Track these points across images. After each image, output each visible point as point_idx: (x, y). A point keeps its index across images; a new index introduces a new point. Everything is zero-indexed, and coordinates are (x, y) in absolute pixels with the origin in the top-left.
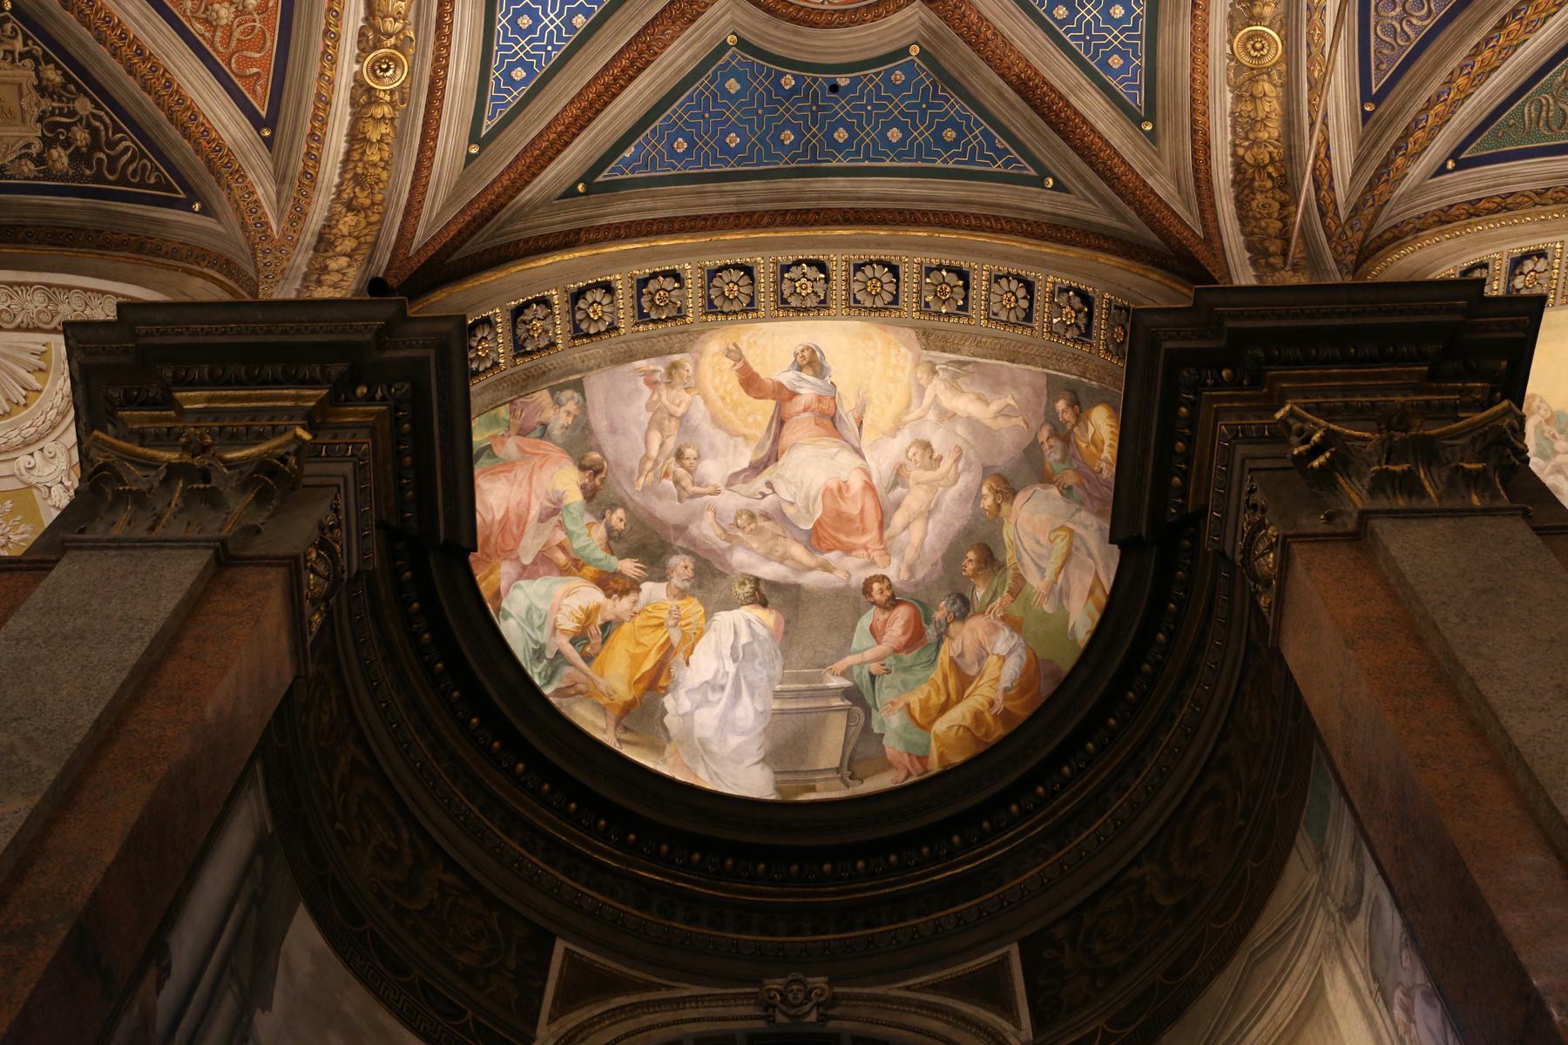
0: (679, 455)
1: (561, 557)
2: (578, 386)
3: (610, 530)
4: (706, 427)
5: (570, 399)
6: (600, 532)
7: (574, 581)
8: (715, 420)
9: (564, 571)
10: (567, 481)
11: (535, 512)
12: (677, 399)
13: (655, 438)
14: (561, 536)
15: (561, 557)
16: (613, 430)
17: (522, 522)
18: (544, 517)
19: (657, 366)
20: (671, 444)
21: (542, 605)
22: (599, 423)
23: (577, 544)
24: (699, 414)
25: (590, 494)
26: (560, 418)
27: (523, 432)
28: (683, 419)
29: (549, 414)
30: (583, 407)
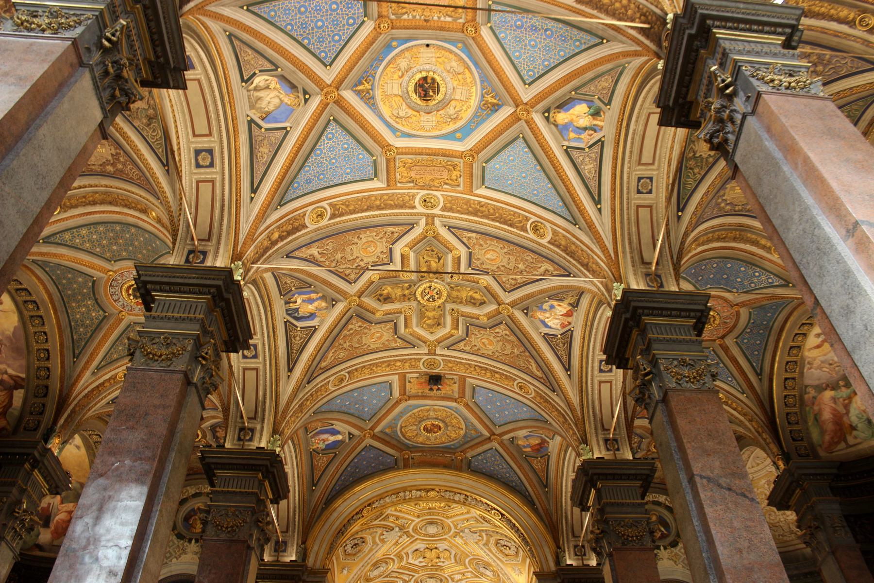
0: (831, 364)
1: (846, 402)
2: (806, 386)
3: (844, 386)
4: (826, 357)
5: (809, 389)
6: (843, 389)
7: (854, 400)
8: (825, 355)
9: (850, 402)
10: (828, 394)
11: (833, 405)
12: (817, 363)
13: (825, 369)
14: (841, 400)
15: (846, 402)
16: (819, 379)
17: (835, 410)
18: (835, 403)
19: (807, 366)
20: (827, 366)
21: (857, 412)
22: (816, 383)
23: (845, 396)
24: (822, 358)
25: (833, 389)
26: (812, 392)
27: (813, 404)
28: (822, 362)
29: (811, 395)
30: (812, 386)
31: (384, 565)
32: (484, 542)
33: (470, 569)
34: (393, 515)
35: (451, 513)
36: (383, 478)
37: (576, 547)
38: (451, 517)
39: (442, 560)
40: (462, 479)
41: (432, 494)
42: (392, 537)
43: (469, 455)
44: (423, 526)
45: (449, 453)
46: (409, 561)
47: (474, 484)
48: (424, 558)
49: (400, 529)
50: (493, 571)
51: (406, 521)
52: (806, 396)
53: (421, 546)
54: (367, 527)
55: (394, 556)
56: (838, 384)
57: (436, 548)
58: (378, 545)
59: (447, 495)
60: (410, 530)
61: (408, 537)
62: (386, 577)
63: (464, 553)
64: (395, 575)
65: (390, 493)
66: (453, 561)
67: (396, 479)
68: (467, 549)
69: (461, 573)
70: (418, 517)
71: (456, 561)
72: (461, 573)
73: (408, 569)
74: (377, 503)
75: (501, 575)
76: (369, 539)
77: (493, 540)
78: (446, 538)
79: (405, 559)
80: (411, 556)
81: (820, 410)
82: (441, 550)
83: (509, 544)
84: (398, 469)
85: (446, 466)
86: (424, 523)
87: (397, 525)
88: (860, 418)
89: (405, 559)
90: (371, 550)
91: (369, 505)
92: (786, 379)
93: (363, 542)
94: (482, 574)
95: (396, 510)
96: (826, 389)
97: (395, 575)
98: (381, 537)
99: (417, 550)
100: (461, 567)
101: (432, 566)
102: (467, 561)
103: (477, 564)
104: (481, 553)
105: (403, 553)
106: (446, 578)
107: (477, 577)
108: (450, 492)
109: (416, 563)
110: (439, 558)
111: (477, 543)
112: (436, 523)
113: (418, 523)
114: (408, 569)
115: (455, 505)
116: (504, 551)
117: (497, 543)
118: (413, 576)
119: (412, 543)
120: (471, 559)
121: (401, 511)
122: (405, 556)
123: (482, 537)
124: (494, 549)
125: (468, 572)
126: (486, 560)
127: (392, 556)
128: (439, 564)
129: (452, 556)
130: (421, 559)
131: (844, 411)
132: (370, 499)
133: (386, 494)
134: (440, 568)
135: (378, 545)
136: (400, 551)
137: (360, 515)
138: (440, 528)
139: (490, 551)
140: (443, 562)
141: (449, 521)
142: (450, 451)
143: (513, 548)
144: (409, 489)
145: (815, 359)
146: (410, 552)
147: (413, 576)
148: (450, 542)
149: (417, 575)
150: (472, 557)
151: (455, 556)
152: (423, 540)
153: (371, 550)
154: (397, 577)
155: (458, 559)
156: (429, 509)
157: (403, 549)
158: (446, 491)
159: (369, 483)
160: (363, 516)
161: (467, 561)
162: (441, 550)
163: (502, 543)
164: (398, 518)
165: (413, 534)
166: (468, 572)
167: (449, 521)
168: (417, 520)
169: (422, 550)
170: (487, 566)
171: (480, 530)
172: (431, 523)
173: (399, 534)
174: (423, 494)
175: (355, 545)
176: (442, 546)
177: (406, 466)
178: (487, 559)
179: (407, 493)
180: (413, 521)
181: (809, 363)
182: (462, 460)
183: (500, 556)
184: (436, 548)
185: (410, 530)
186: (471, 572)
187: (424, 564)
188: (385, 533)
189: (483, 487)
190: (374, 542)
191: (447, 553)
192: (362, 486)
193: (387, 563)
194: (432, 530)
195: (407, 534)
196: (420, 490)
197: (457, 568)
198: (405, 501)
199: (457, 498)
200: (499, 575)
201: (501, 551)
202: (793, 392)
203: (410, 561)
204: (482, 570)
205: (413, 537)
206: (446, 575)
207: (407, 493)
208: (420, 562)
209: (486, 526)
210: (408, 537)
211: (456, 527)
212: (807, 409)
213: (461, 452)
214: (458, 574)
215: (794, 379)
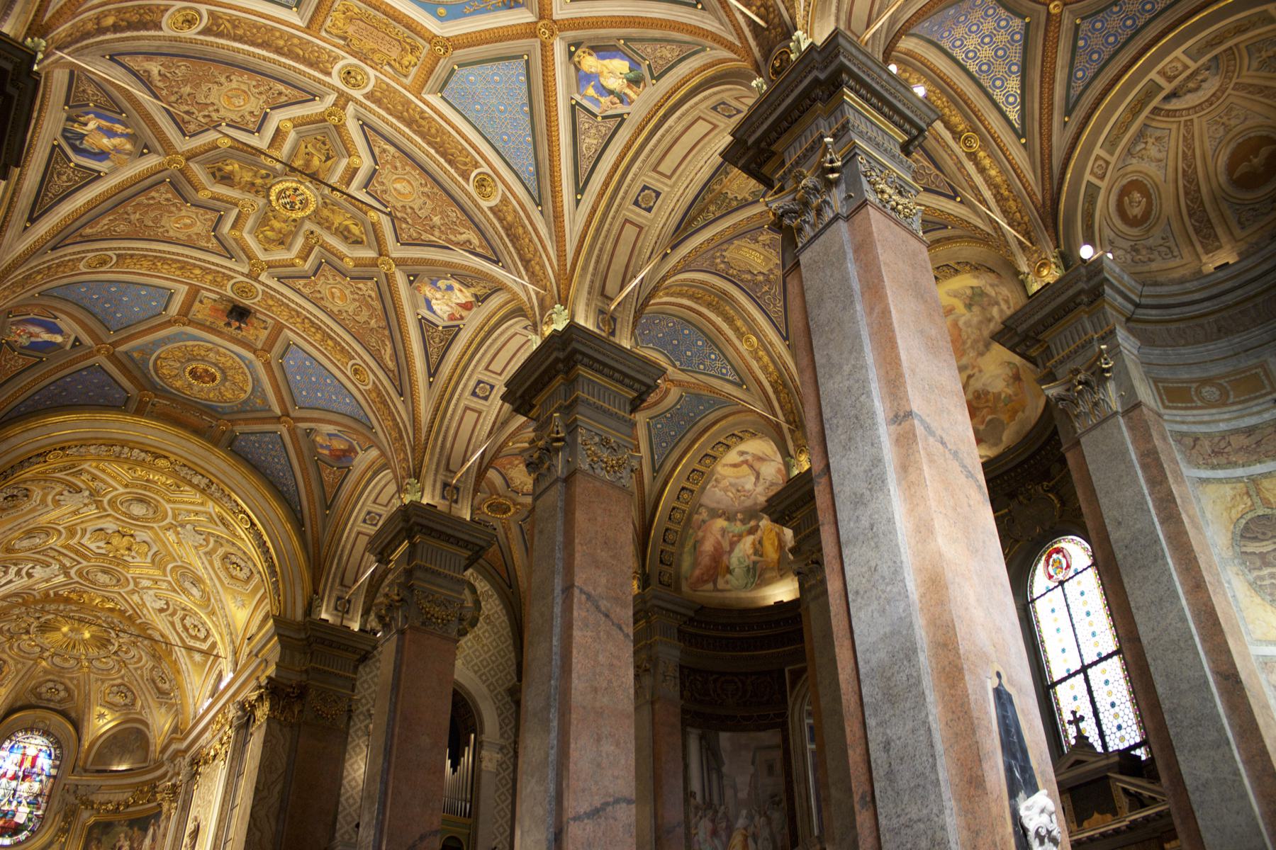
0: (738, 491)
1: (735, 539)
2: (701, 505)
3: (741, 520)
4: (737, 481)
5: (703, 510)
6: (738, 523)
7: (743, 540)
8: (737, 478)
9: (739, 541)
10: (721, 523)
11: (720, 537)
12: (725, 483)
13: (730, 494)
14: (731, 535)
15: (735, 539)
16: (718, 503)
17: (719, 543)
18: (723, 536)
19: (713, 483)
20: (734, 491)
21: (741, 555)
22: (714, 505)
23: (736, 532)
24: (733, 480)
25: (728, 519)
26: (704, 514)
27: (699, 528)
28: (731, 484)
29: (701, 518)
30: (706, 507)
31: (43, 536)
32: (207, 549)
33: (169, 578)
34: (89, 473)
35: (177, 497)
36: (98, 416)
37: (339, 598)
38: (174, 502)
39: (133, 554)
40: (213, 457)
41: (161, 463)
42: (71, 503)
43: (238, 429)
44: (127, 501)
45: (211, 416)
46: (82, 541)
47: (228, 469)
48: (108, 543)
49: (91, 495)
50: (203, 591)
51: (104, 487)
52: (696, 517)
53: (110, 526)
54: (44, 478)
55: (65, 528)
56: (736, 515)
57: (132, 536)
58: (47, 506)
59: (184, 471)
60: (105, 500)
61: (97, 508)
62: (38, 553)
63: (170, 554)
64: (55, 554)
65: (101, 442)
66: (149, 560)
67: (117, 424)
68: (175, 549)
69: (153, 580)
70: (126, 486)
71: (153, 561)
72: (153, 580)
73: (77, 552)
74: (74, 450)
75: (212, 600)
76: (37, 494)
77: (221, 551)
78: (153, 528)
79: (78, 536)
80: (88, 535)
81: (704, 537)
82: (138, 540)
83: (243, 564)
84: (126, 412)
85: (197, 432)
86: (129, 497)
87: (89, 488)
88: (740, 563)
89: (78, 536)
90: (33, 510)
91: (62, 449)
92: (683, 489)
93: (27, 496)
94: (184, 590)
95: (97, 467)
96: (720, 517)
97: (52, 553)
98: (57, 497)
99: (101, 530)
100: (157, 572)
101: (114, 557)
102: (170, 567)
103: (183, 575)
104: (198, 565)
105: (78, 528)
106: (127, 580)
107: (175, 591)
108: (189, 468)
109: (93, 546)
110: (129, 549)
111: (196, 547)
112: (148, 503)
113: (122, 494)
114: (77, 552)
115: (187, 488)
116: (231, 570)
117: (225, 557)
118: (79, 563)
119: (98, 518)
120: (177, 566)
121: (104, 471)
122: (79, 532)
123: (208, 543)
124: (217, 564)
125: (164, 581)
126: (200, 574)
127: (60, 528)
128: (125, 558)
129: (150, 554)
130: (102, 544)
131: (728, 549)
132: (66, 441)
133: (94, 442)
134: (126, 564)
135: (47, 506)
136: (76, 524)
137: (42, 459)
138: (151, 511)
139: (211, 564)
140: (133, 558)
141: (168, 507)
142: (213, 414)
143: (246, 571)
144: (131, 444)
145: (724, 477)
146: (89, 530)
147: (79, 563)
148: (157, 534)
149: (85, 563)
150: (180, 564)
151: (155, 554)
152: (118, 519)
153: (33, 510)
154: (53, 558)
155: (157, 559)
156: (148, 481)
157: (82, 522)
158: (185, 466)
159: (73, 417)
160: (45, 462)
161: (170, 567)
162: (138, 540)
163: (234, 559)
164: (94, 478)
165: (107, 507)
166: (164, 581)
167: (168, 507)
168: (122, 490)
169: (110, 532)
170: (197, 581)
171: (209, 533)
172: (141, 500)
173: (86, 501)
174: (149, 458)
175: (13, 496)
176: (142, 535)
177: (140, 411)
178: (202, 572)
179: (126, 450)
180: (116, 489)
181: (716, 480)
182: (224, 432)
183: (222, 574)
184: (132, 536)
185: (105, 500)
186: (169, 583)
187: (103, 551)
188: (66, 493)
189: (239, 478)
190: (43, 502)
191: (145, 548)
192: (61, 418)
193: (48, 534)
194: (138, 510)
195: (99, 505)
196: (146, 452)
197: (151, 572)
198: (118, 459)
199: (196, 480)
200: (209, 599)
201: (227, 569)
202: (683, 507)
203: (85, 541)
204: (187, 585)
205: (105, 510)
206: (129, 576)
207: (126, 450)
208: (99, 548)
209: (221, 531)
210: (97, 508)
211: (175, 517)
212: (691, 531)
213: (229, 421)
214: (148, 579)
215: (692, 491)
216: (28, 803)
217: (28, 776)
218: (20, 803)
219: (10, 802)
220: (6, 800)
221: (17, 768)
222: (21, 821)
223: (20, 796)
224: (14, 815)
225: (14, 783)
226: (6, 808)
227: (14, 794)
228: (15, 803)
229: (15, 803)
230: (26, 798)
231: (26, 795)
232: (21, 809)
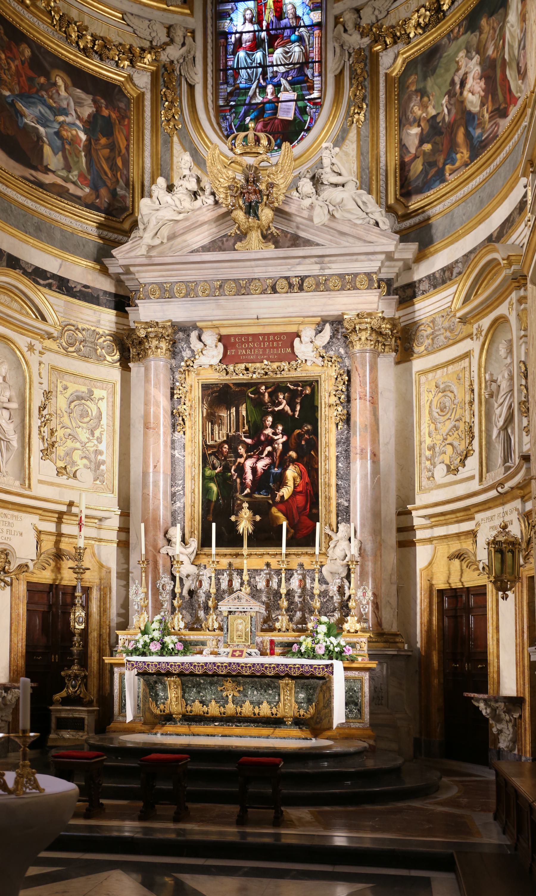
216: (291, 83)
217: (276, 37)
218: (278, 86)
219: (262, 89)
220: (254, 86)
221: (256, 27)
222: (290, 117)
223: (275, 74)
224: (275, 110)
225: (258, 55)
226: (259, 99)
227: (264, 73)
228: (270, 89)
229: (270, 89)
230: (285, 75)
231: (282, 69)
232: (283, 96)
